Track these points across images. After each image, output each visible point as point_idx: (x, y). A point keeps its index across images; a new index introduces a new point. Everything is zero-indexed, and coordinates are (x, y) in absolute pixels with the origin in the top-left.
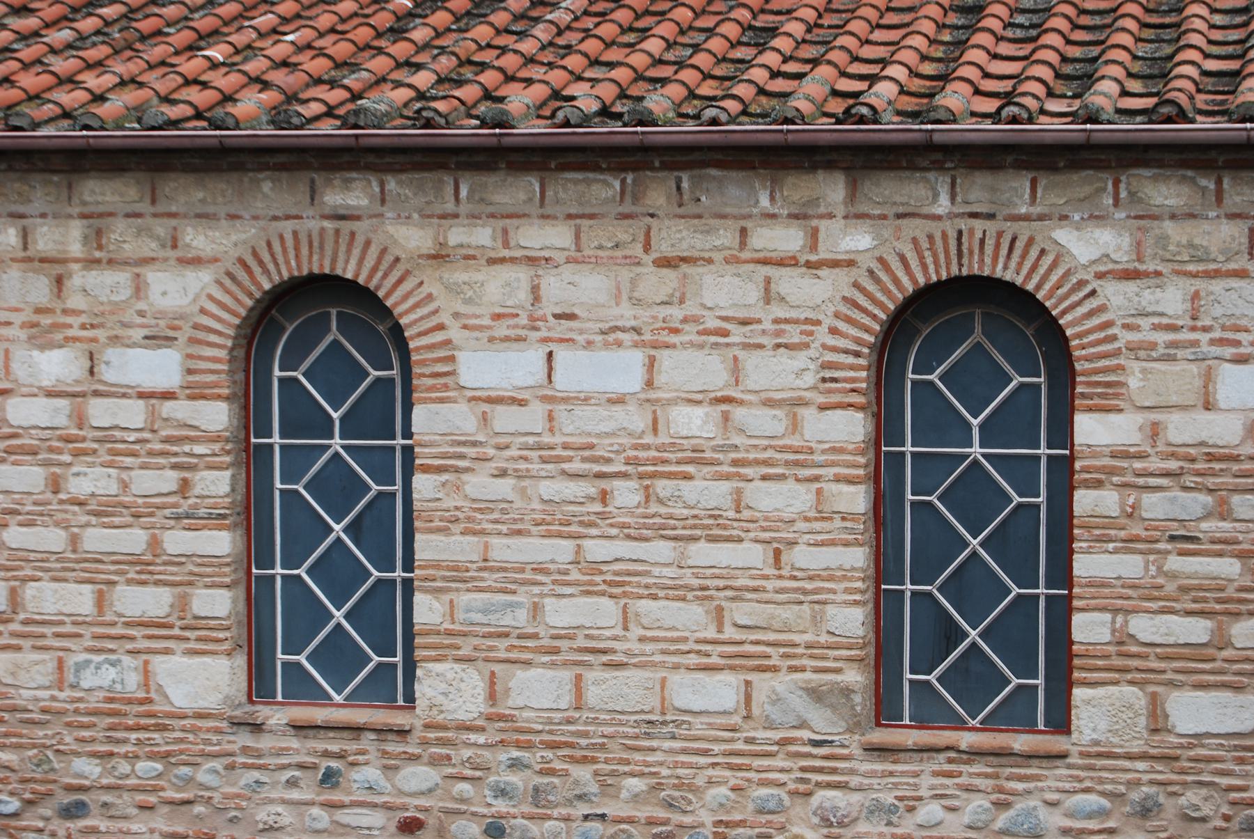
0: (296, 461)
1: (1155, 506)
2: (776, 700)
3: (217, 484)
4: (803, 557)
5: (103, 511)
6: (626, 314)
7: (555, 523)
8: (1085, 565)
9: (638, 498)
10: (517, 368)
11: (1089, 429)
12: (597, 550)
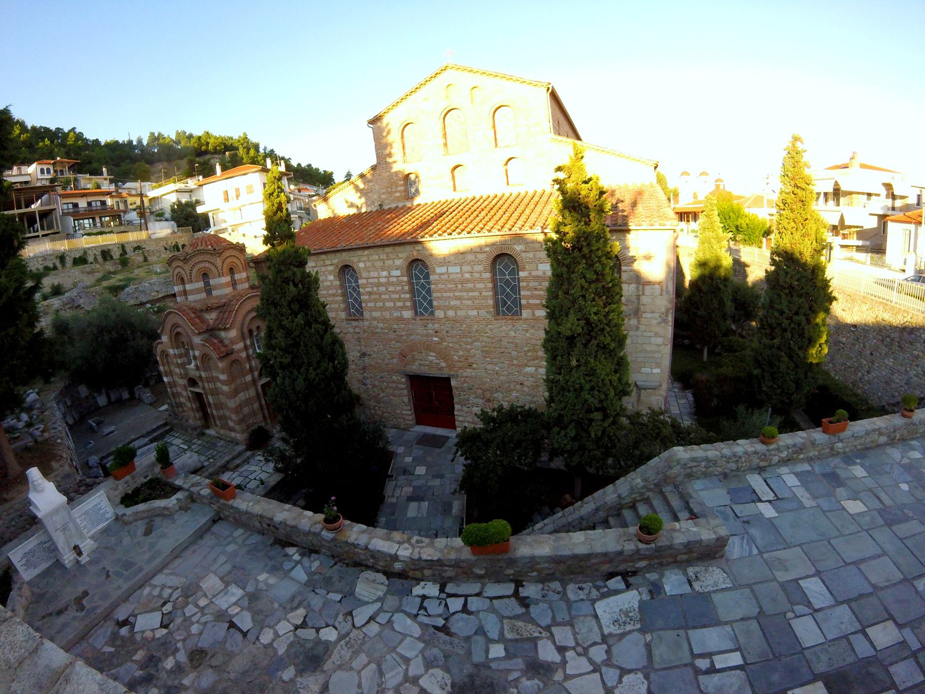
0: (417, 284)
3: (407, 288)
4: (484, 294)
5: (393, 292)
6: (457, 261)
7: (450, 290)
8: (522, 293)
12: (457, 294)
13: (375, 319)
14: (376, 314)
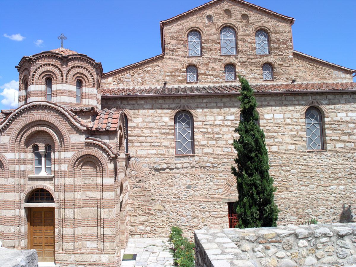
1: (333, 126)
2: (299, 147)
4: (300, 133)
5: (226, 133)
6: (281, 110)
9: (283, 128)
10: (271, 116)
11: (326, 119)
12: (280, 134)
13: (206, 154)
14: (206, 150)
